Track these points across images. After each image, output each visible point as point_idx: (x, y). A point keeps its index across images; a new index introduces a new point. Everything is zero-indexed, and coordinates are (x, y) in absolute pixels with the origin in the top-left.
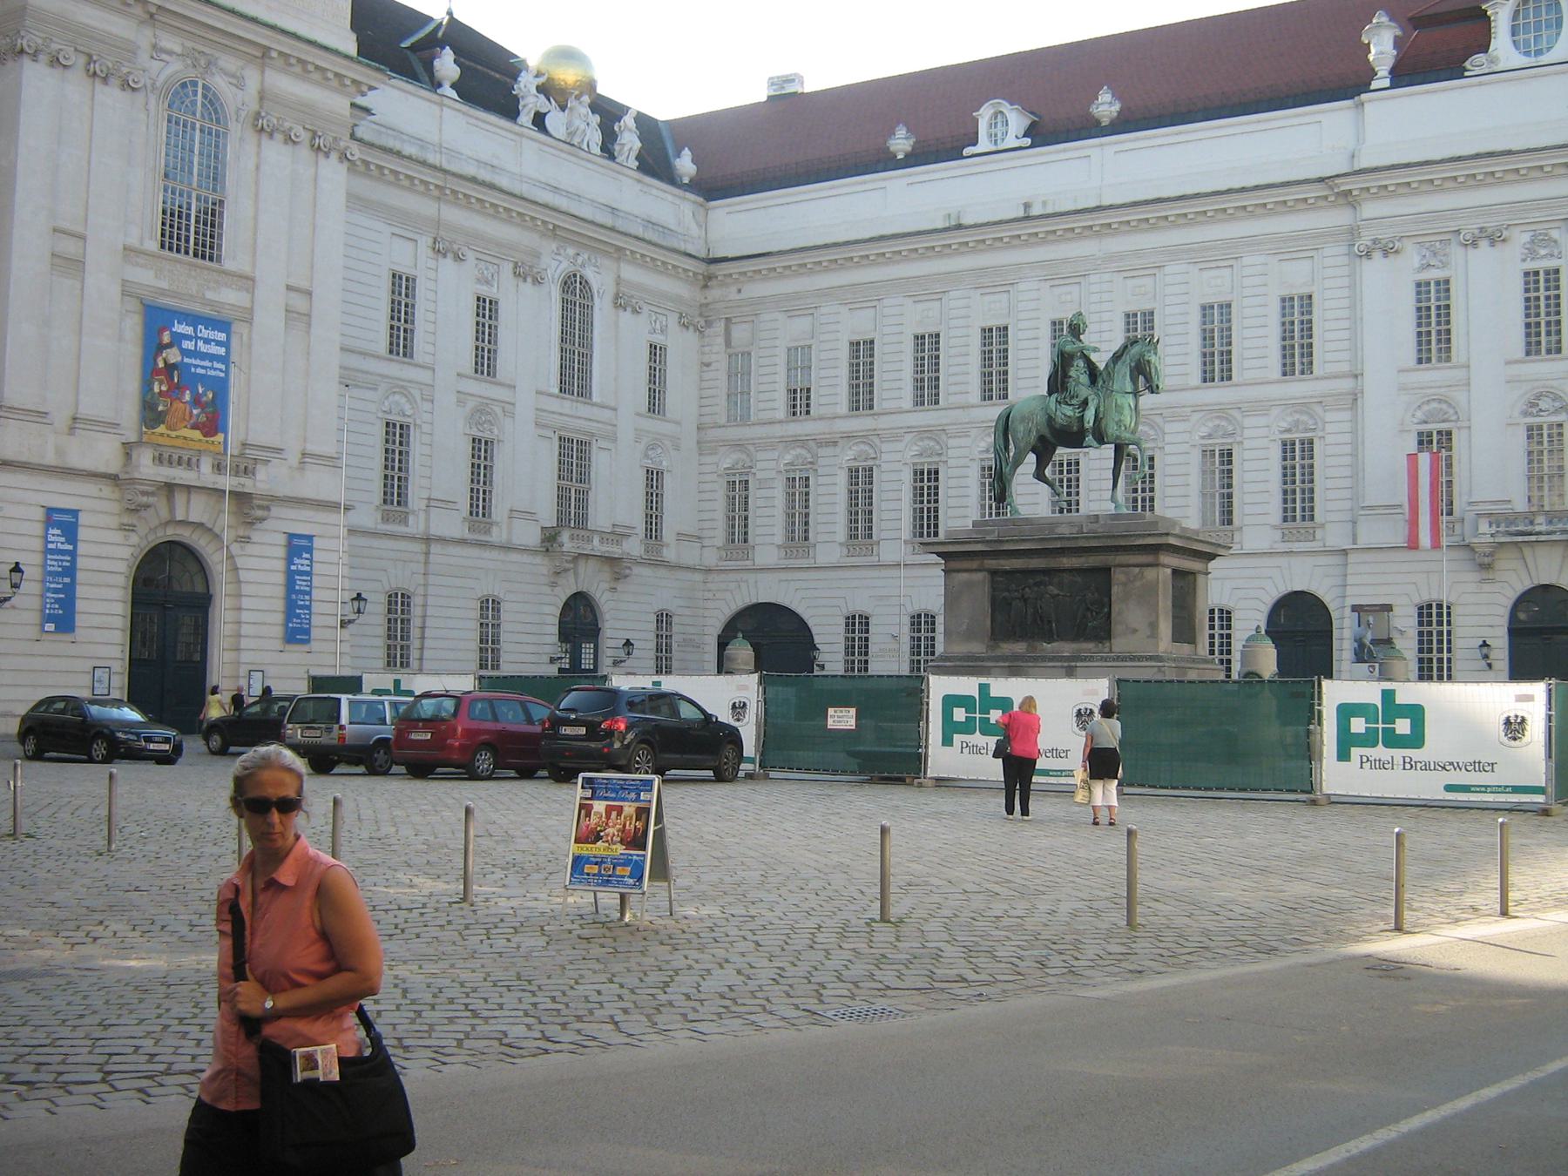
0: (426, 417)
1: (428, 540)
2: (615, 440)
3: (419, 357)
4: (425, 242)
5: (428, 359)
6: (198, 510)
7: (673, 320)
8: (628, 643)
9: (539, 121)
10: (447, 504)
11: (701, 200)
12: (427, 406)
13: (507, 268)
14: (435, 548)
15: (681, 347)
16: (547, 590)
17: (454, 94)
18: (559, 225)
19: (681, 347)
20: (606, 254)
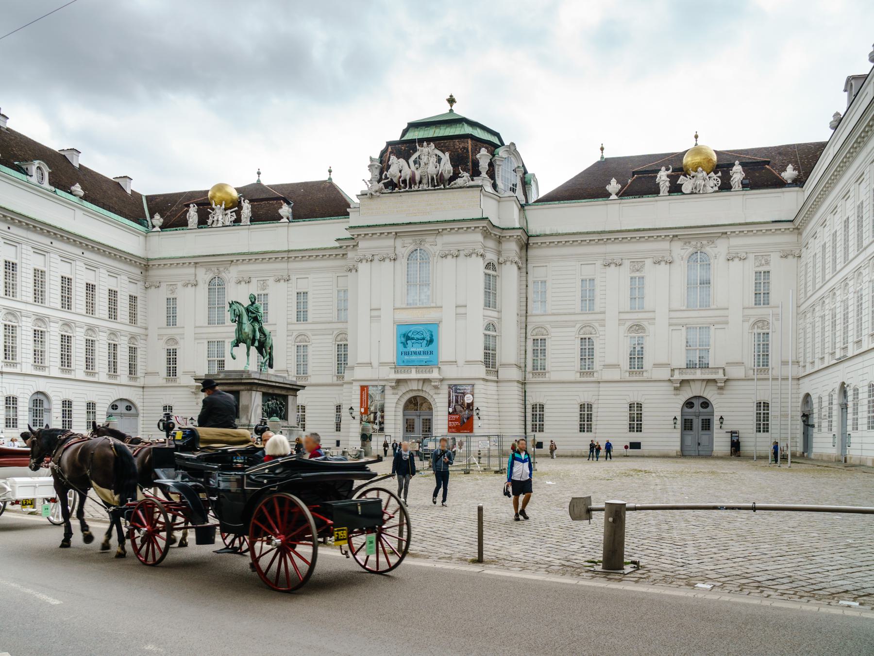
0: (601, 333)
1: (599, 382)
2: (727, 323)
3: (597, 309)
4: (599, 263)
5: (602, 310)
6: (414, 386)
7: (775, 258)
8: (721, 418)
9: (675, 189)
10: (616, 366)
11: (797, 189)
12: (602, 328)
13: (649, 262)
14: (601, 385)
15: (778, 267)
16: (674, 397)
17: (616, 197)
18: (675, 234)
19: (778, 267)
20: (719, 237)
